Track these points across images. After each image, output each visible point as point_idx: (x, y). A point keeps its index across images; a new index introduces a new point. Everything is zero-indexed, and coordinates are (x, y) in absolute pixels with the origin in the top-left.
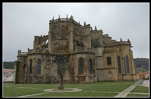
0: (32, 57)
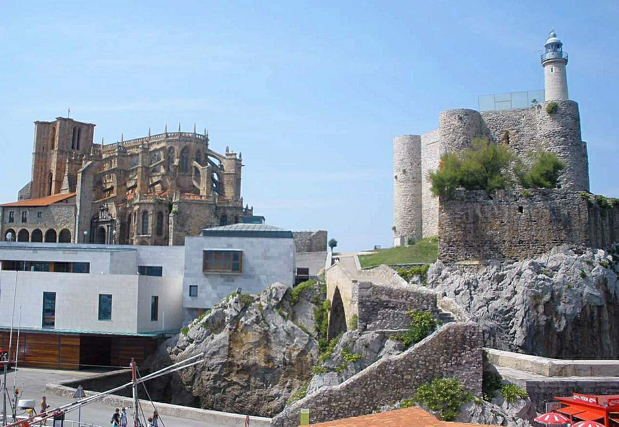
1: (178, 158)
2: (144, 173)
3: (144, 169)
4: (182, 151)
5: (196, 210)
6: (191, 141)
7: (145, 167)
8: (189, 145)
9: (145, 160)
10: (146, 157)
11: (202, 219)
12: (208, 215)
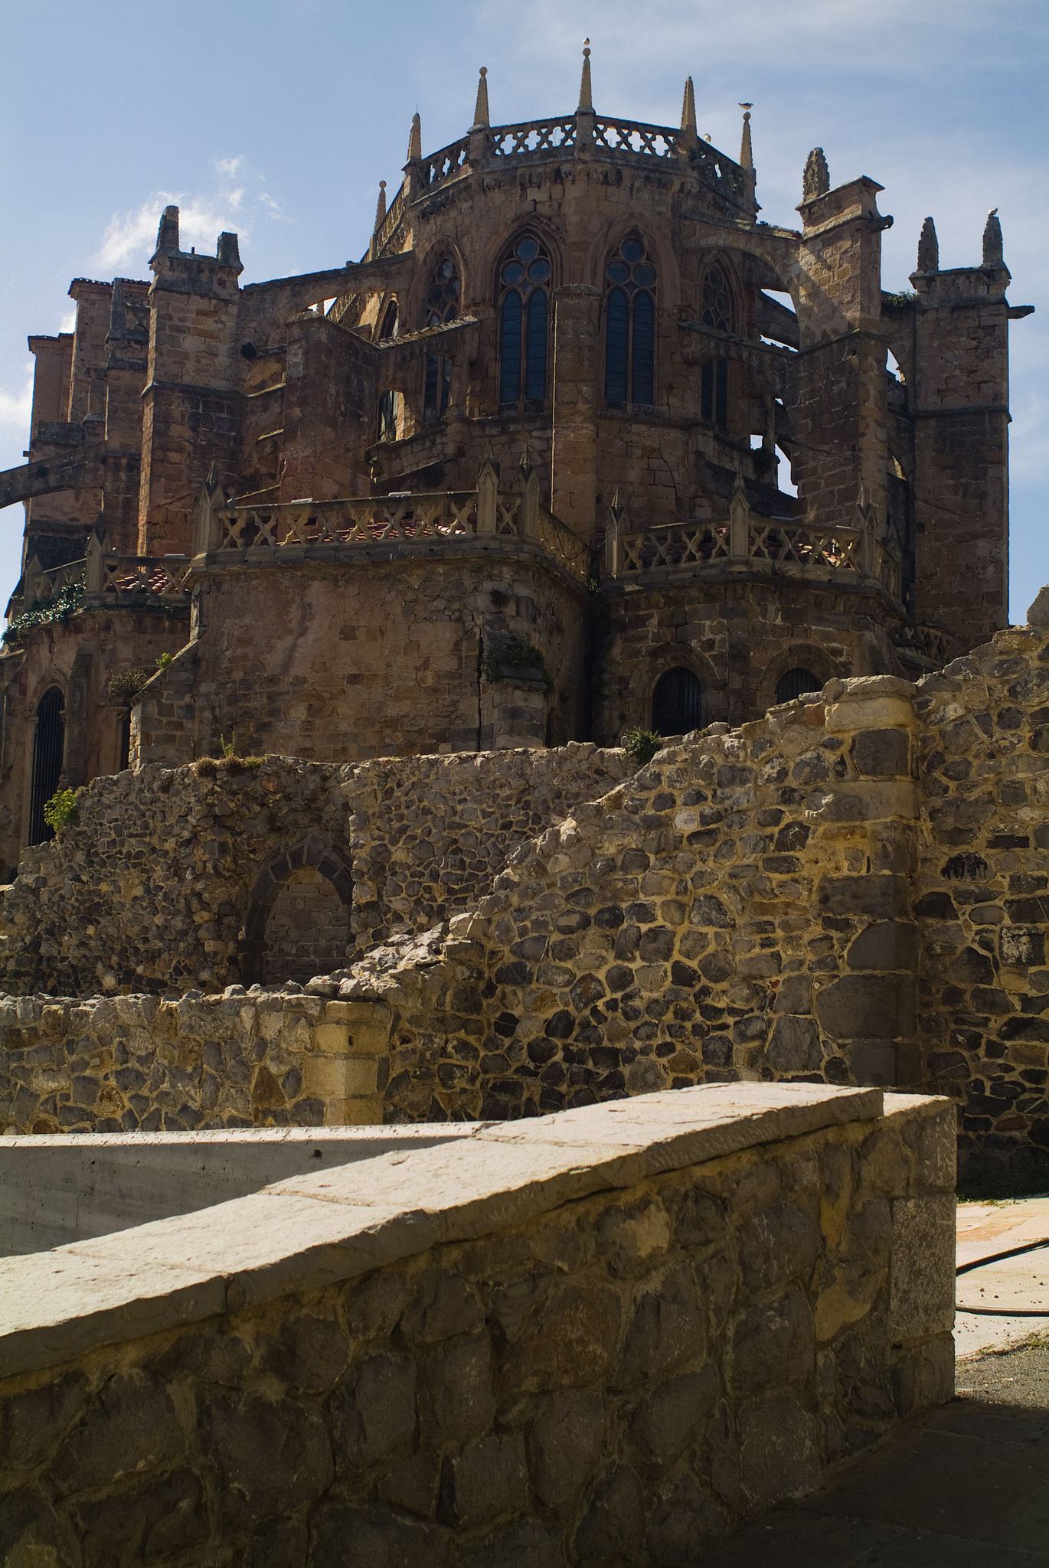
0: (826, 637)
1: (474, 305)
2: (180, 431)
3: (178, 407)
4: (507, 254)
5: (348, 634)
6: (558, 177)
7: (192, 393)
8: (544, 209)
9: (190, 344)
10: (209, 324)
11: (392, 711)
12: (452, 664)
